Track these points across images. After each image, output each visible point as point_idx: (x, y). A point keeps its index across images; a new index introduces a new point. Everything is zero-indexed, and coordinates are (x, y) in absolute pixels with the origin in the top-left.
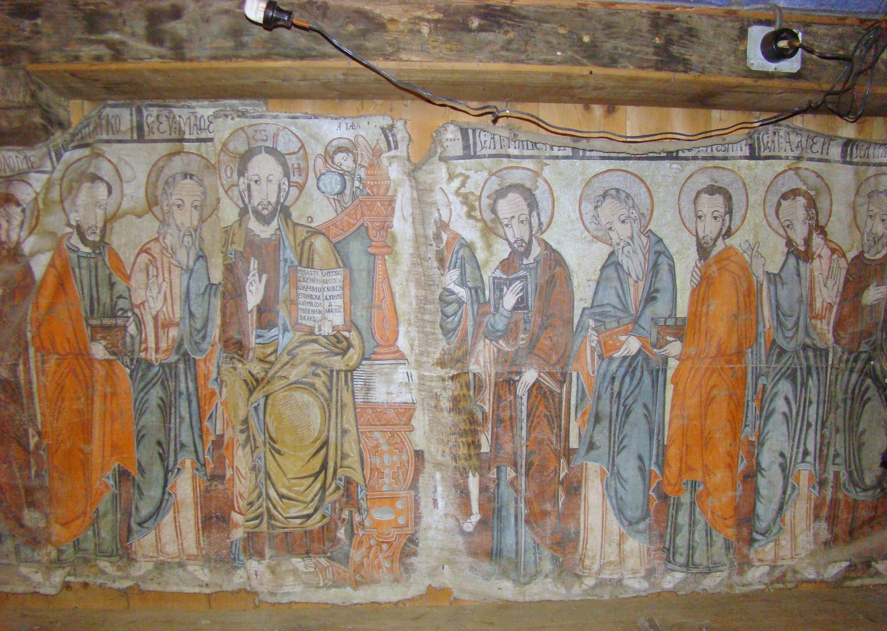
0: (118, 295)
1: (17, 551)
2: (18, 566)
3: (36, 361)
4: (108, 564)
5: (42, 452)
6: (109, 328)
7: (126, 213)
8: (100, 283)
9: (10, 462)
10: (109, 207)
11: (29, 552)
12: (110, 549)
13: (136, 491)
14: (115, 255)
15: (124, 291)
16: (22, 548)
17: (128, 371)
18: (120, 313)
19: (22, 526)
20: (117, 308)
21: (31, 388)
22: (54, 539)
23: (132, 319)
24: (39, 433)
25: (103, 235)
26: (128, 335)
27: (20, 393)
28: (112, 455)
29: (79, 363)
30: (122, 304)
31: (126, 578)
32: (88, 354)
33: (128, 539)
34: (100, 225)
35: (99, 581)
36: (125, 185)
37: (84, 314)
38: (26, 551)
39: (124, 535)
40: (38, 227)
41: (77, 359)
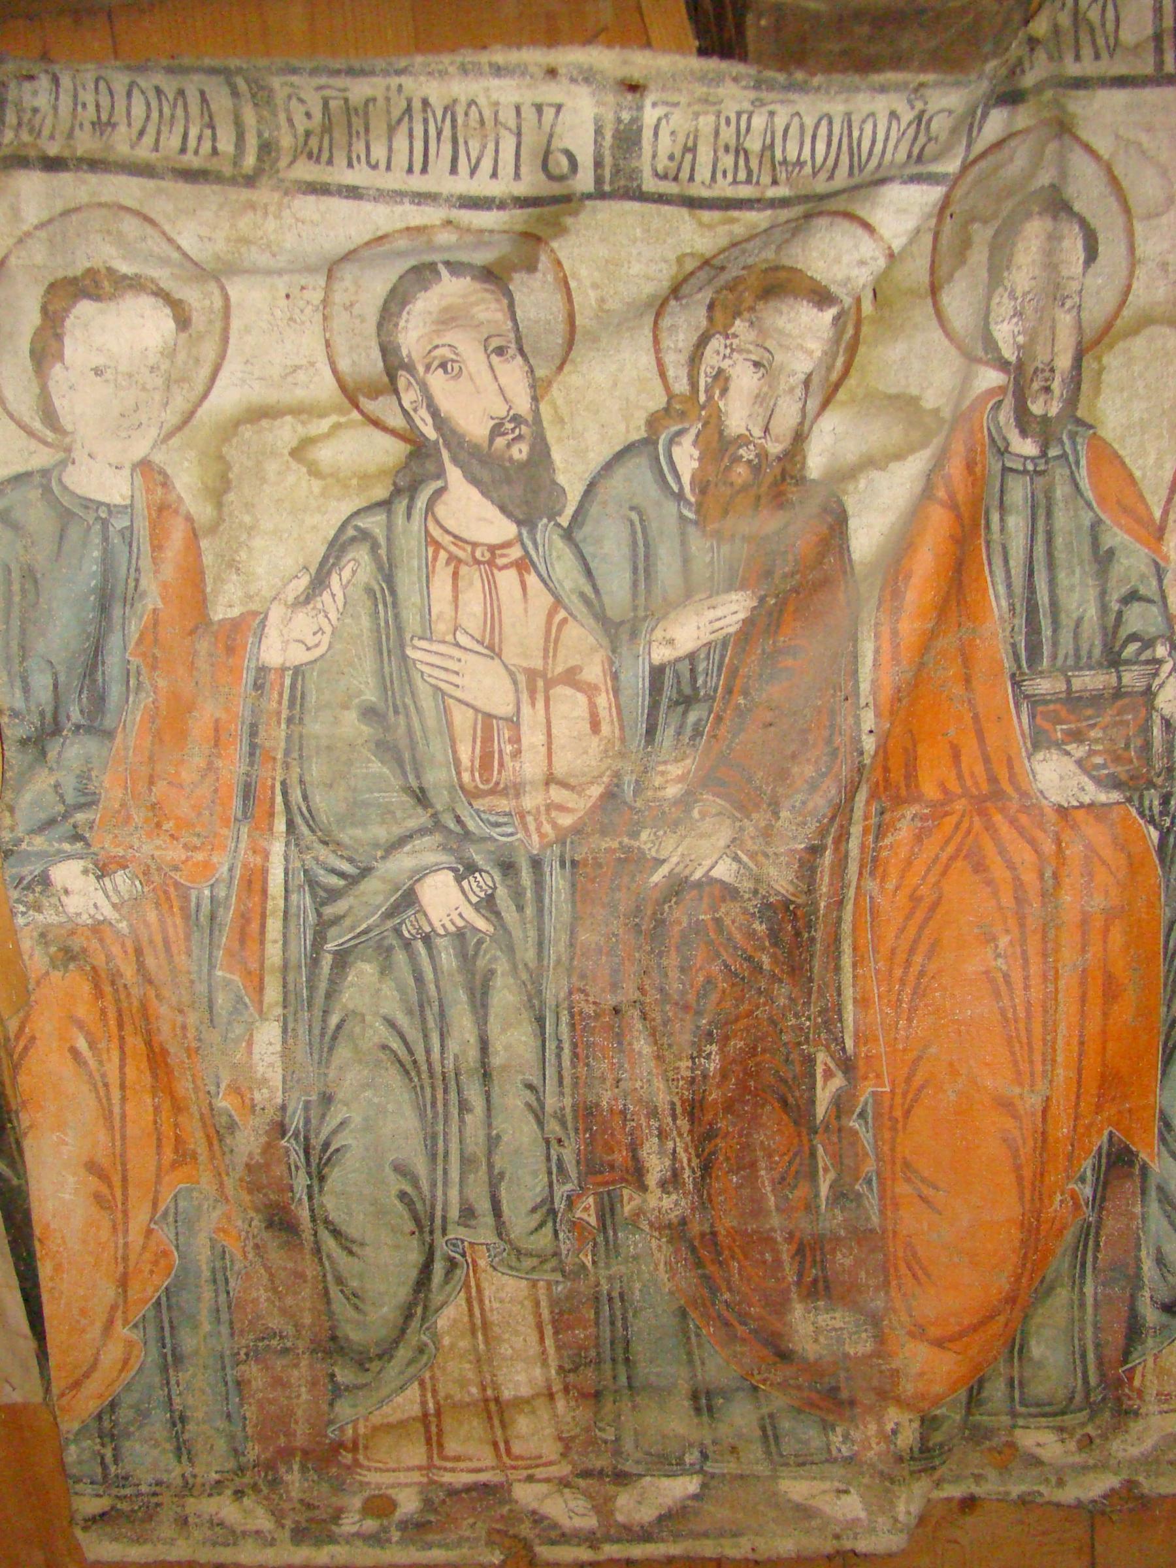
0: (1124, 590)
1: (769, 1434)
2: (774, 1477)
3: (866, 831)
4: (1049, 1437)
5: (854, 1124)
6: (1096, 700)
7: (1145, 321)
8: (1061, 555)
9: (753, 1165)
10: (1089, 303)
11: (812, 1435)
12: (1061, 1393)
13: (1154, 1207)
14: (1106, 457)
15: (1143, 577)
16: (786, 1424)
17: (1155, 835)
18: (1132, 648)
19: (784, 1356)
20: (1123, 633)
21: (839, 920)
22: (908, 1388)
23: (1167, 667)
24: (847, 1066)
25: (1072, 401)
26: (1156, 718)
27: (812, 940)
28: (1099, 1108)
29: (990, 827)
30: (1138, 619)
31: (1102, 1466)
32: (1024, 794)
33: (1126, 1355)
34: (1064, 362)
35: (1016, 1490)
36: (1138, 227)
37: (1008, 664)
38: (804, 1433)
39: (1115, 1337)
40: (851, 382)
41: (983, 813)
